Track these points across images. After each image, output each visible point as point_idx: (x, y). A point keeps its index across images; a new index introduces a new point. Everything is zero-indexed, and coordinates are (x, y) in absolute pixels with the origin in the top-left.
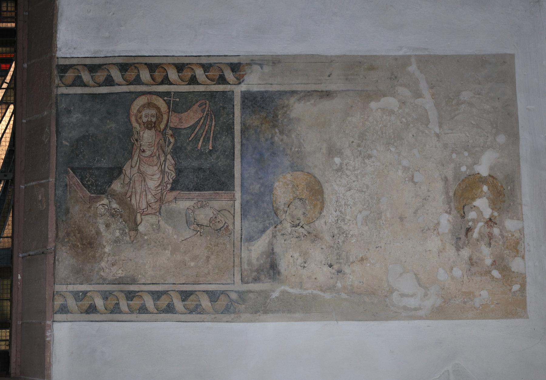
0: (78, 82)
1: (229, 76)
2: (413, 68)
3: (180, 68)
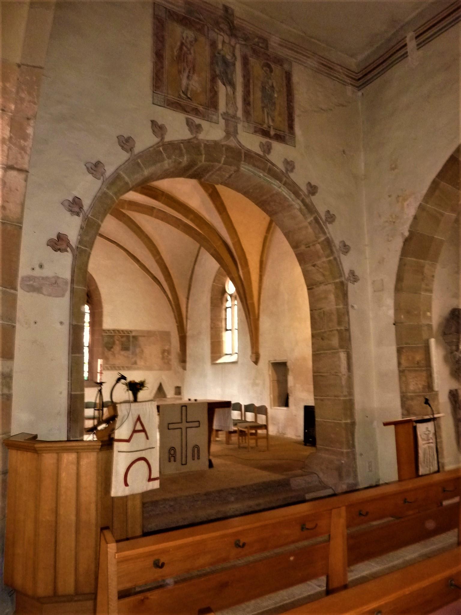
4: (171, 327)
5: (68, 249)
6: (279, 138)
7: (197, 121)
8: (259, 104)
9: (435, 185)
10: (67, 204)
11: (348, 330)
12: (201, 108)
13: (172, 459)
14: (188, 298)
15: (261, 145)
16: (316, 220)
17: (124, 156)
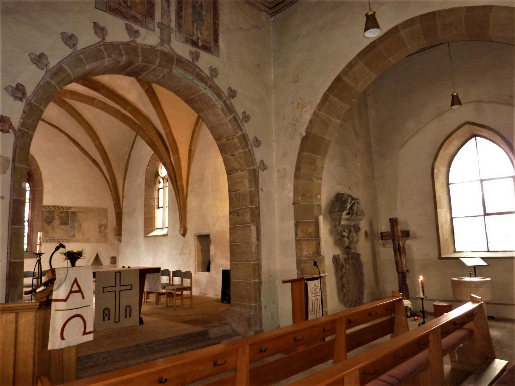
0: (46, 209)
4: (109, 204)
5: (11, 130)
6: (206, 48)
7: (136, 27)
8: (190, 19)
9: (325, 98)
10: (10, 89)
11: (258, 208)
12: (139, 16)
13: (106, 318)
14: (124, 179)
15: (191, 53)
16: (235, 119)
17: (68, 51)
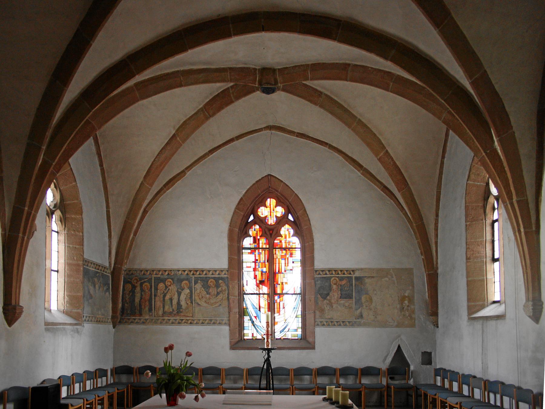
1: (352, 273)
2: (391, 271)
3: (341, 271)
4: (413, 261)
